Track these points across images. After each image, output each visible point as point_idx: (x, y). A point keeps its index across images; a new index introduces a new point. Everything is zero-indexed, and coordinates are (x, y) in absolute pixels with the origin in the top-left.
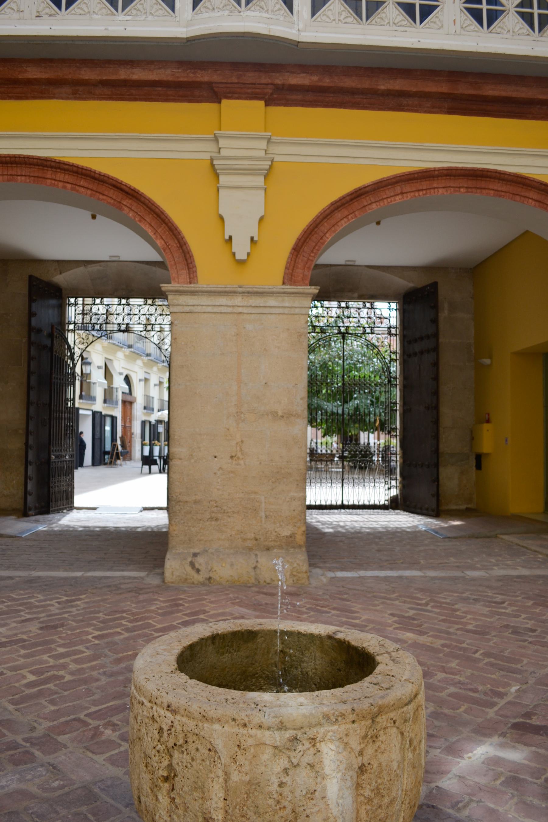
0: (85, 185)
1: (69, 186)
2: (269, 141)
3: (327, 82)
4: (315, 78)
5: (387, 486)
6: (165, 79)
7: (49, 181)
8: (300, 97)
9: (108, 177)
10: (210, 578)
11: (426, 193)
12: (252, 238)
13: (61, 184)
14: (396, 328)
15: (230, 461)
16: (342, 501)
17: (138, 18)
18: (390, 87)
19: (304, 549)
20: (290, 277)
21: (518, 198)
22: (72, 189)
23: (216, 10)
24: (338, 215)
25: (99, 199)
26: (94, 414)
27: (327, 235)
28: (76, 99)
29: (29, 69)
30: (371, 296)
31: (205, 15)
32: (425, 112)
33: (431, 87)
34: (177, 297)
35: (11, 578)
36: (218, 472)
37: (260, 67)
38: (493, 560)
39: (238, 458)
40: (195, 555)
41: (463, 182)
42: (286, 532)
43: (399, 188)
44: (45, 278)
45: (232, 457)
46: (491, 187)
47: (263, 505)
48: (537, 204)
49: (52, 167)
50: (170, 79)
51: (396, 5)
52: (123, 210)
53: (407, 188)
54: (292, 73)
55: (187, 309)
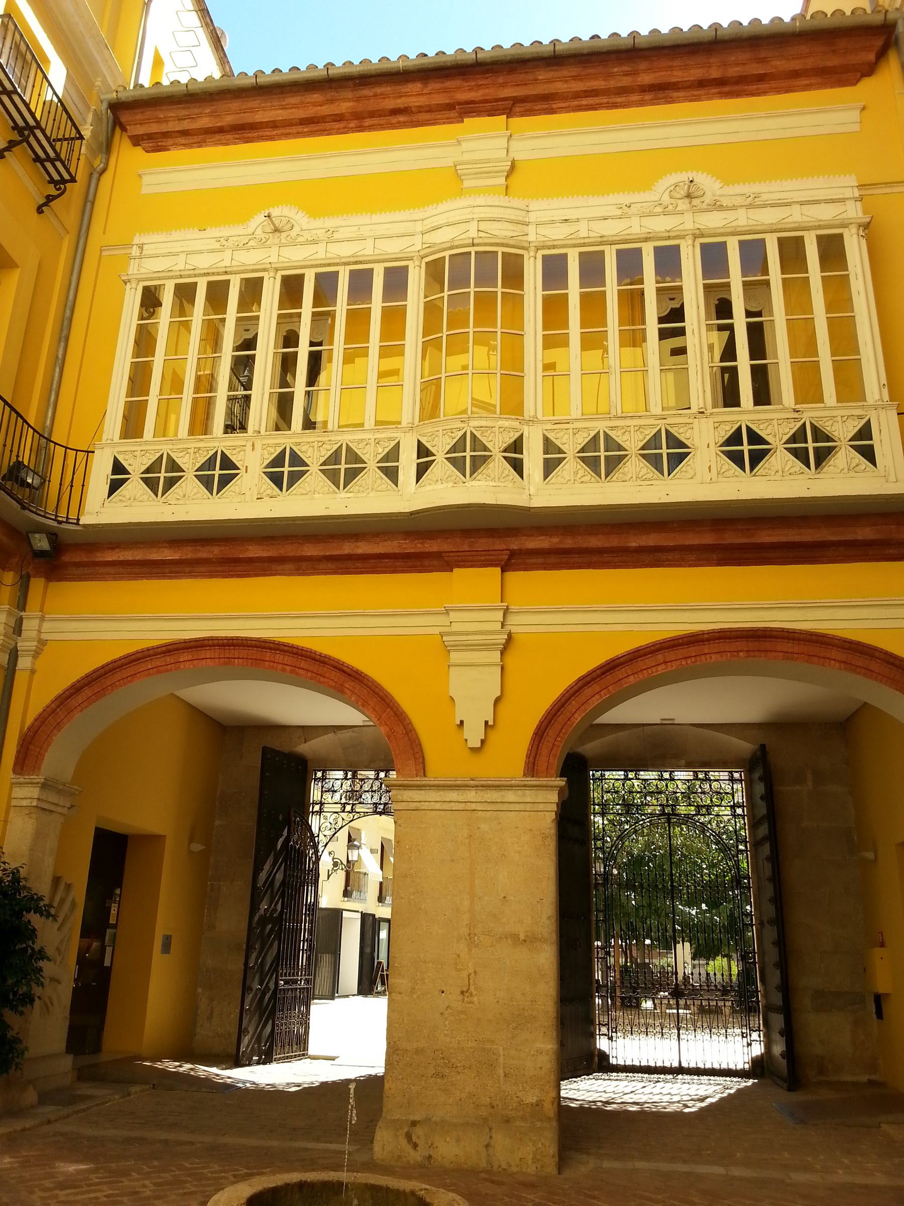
0: (306, 667)
1: (288, 668)
3: (569, 543)
4: (555, 540)
5: (745, 1039)
6: (391, 551)
7: (267, 663)
8: (541, 560)
9: (329, 658)
10: (430, 1157)
11: (696, 661)
12: (486, 722)
13: (280, 666)
14: (744, 806)
15: (461, 997)
16: (680, 1062)
17: (359, 495)
18: (643, 543)
19: (555, 1124)
20: (532, 768)
21: (815, 659)
22: (292, 672)
23: (440, 482)
24: (588, 691)
25: (319, 682)
26: (364, 916)
27: (576, 715)
29: (250, 548)
30: (703, 761)
31: (429, 488)
32: (690, 566)
34: (401, 792)
35: (192, 1143)
36: (446, 1012)
37: (493, 532)
38: (846, 1161)
39: (471, 994)
40: (414, 1124)
41: (741, 645)
42: (531, 1098)
43: (661, 656)
44: (286, 750)
45: (462, 993)
46: (779, 649)
47: (502, 1057)
48: (842, 666)
49: (271, 649)
51: (640, 458)
52: (345, 693)
53: (671, 655)
54: (528, 536)
55: (413, 806)
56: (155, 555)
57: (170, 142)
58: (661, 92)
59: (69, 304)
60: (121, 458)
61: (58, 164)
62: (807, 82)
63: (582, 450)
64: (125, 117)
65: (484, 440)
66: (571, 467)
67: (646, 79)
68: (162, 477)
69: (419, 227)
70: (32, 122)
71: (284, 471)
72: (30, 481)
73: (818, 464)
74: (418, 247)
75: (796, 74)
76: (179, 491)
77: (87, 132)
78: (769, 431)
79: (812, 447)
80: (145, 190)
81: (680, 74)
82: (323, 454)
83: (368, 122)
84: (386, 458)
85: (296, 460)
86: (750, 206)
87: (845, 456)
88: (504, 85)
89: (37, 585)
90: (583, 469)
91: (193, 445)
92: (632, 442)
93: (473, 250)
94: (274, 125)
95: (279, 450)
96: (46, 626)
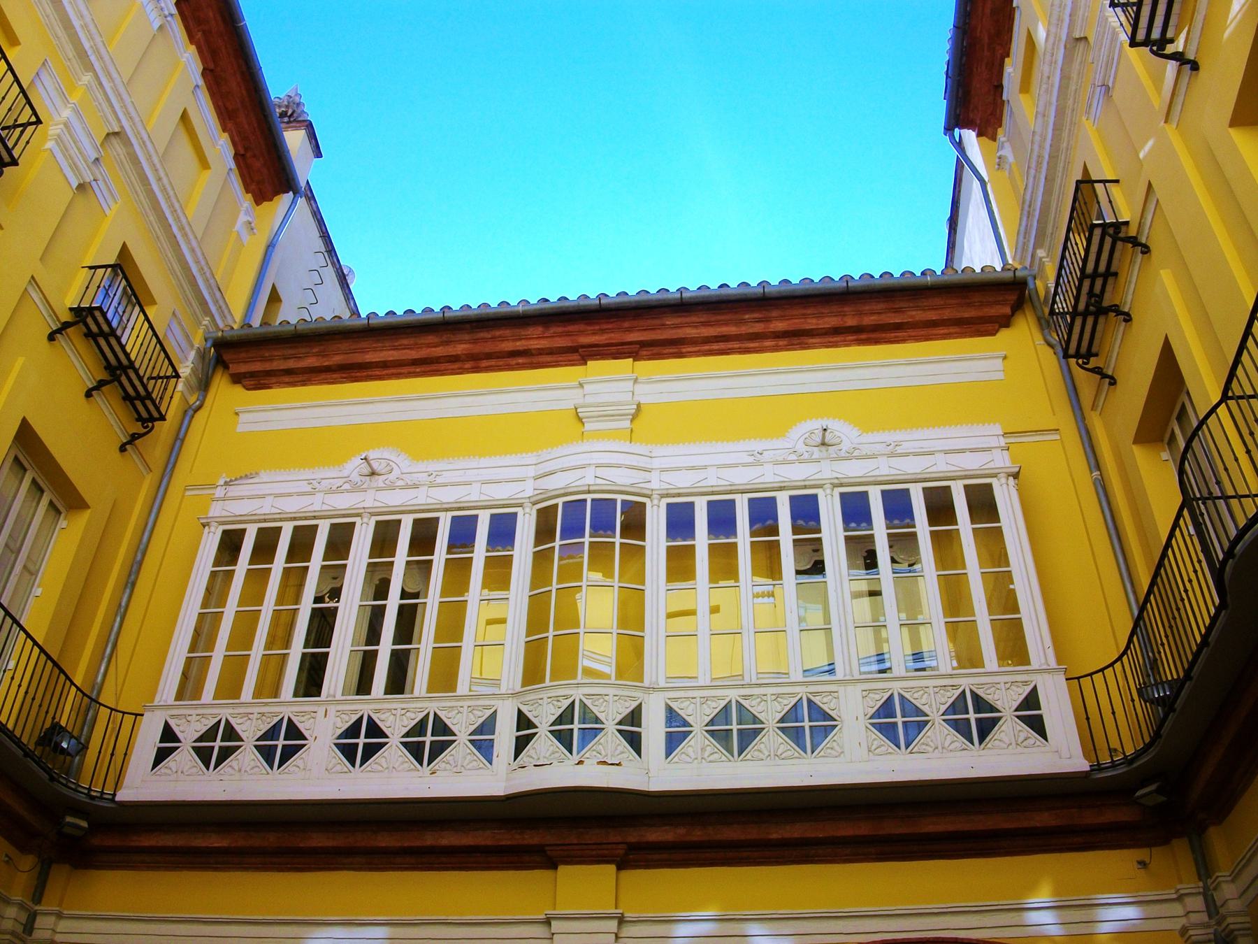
2: (621, 920)
3: (697, 834)
4: (681, 831)
6: (483, 843)
28: (371, 870)
33: (846, 829)
50: (489, 843)
56: (199, 841)
57: (274, 380)
58: (796, 339)
59: (142, 547)
60: (172, 723)
61: (148, 403)
62: (946, 331)
63: (712, 722)
64: (227, 357)
65: (595, 710)
66: (699, 740)
67: (780, 326)
68: (217, 746)
69: (531, 471)
70: (125, 362)
71: (361, 742)
72: (65, 745)
73: (982, 738)
74: (529, 492)
76: (234, 764)
77: (185, 370)
78: (923, 701)
79: (973, 717)
80: (240, 429)
81: (814, 321)
82: (406, 723)
83: (484, 363)
84: (480, 730)
85: (375, 730)
86: (892, 455)
87: (1010, 729)
88: (630, 330)
89: (59, 874)
90: (712, 745)
91: (256, 710)
92: (770, 712)
93: (589, 497)
94: (385, 365)
95: (355, 718)
96: (64, 925)
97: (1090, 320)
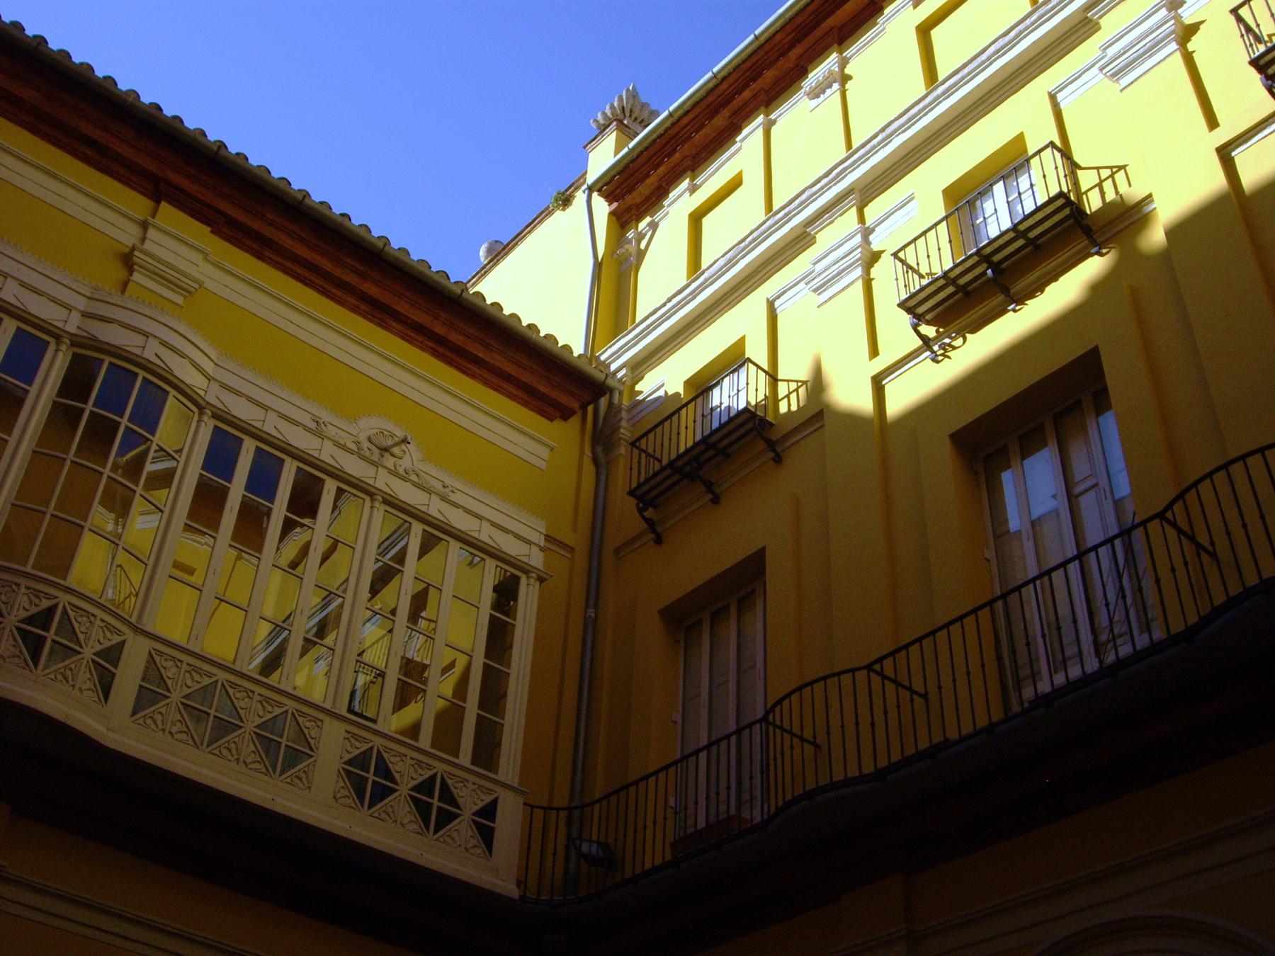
62: (514, 391)
69: (81, 303)
75: (508, 378)
86: (444, 499)
97: (677, 477)
